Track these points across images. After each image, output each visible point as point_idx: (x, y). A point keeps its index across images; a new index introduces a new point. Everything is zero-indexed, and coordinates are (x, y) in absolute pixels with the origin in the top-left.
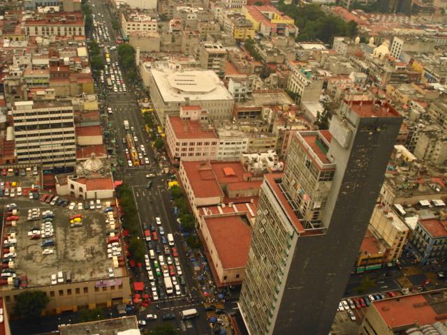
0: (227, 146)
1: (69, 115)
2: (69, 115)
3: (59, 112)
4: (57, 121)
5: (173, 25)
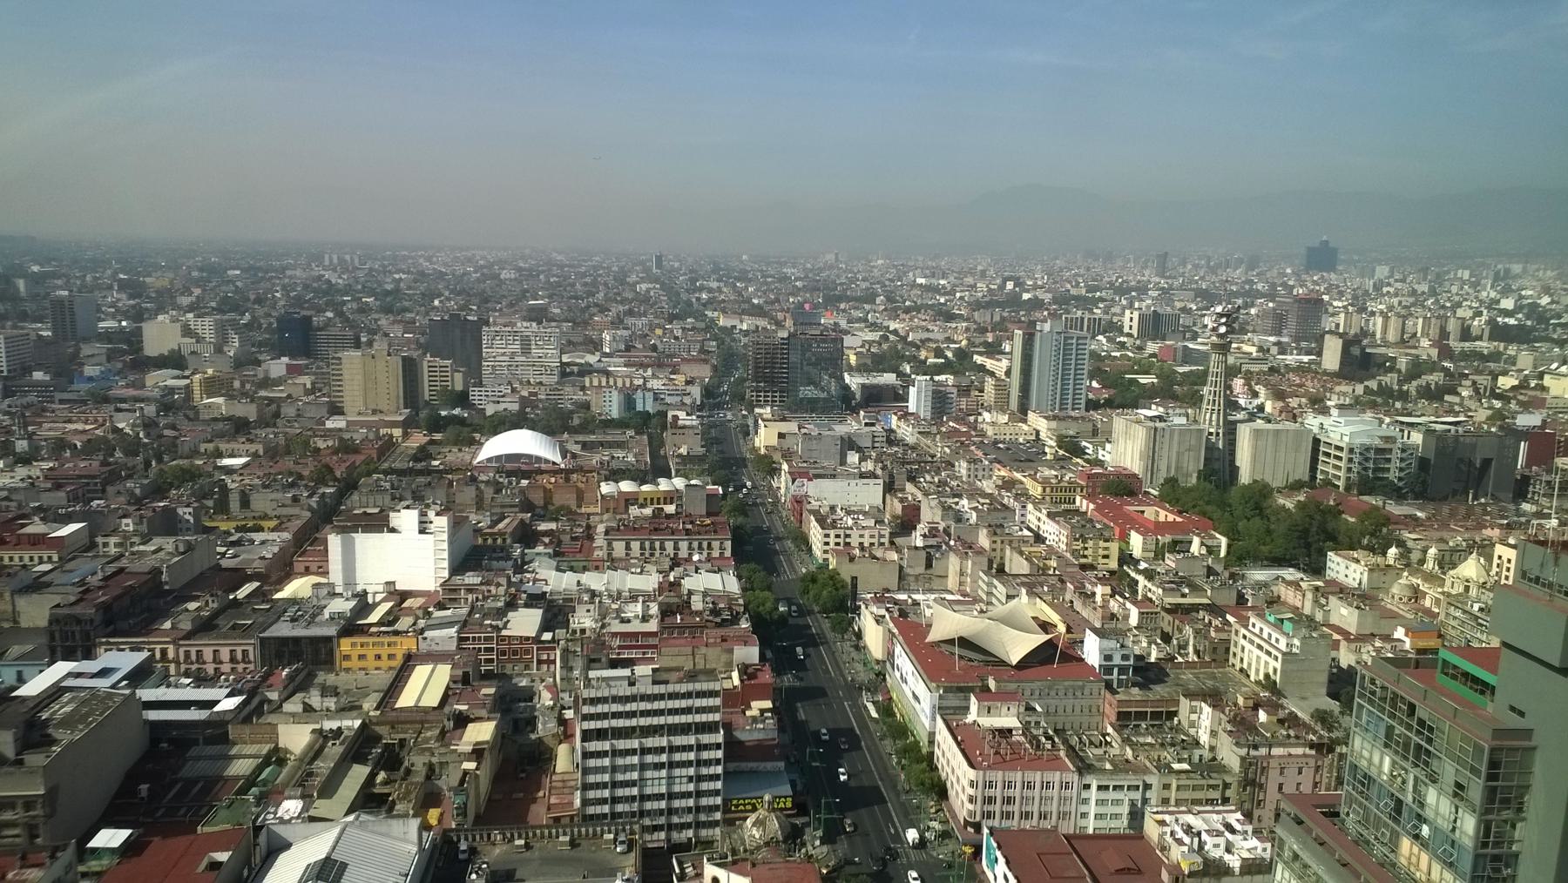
0: (1103, 795)
1: (711, 702)
2: (711, 702)
3: (688, 695)
4: (683, 719)
5: (924, 536)
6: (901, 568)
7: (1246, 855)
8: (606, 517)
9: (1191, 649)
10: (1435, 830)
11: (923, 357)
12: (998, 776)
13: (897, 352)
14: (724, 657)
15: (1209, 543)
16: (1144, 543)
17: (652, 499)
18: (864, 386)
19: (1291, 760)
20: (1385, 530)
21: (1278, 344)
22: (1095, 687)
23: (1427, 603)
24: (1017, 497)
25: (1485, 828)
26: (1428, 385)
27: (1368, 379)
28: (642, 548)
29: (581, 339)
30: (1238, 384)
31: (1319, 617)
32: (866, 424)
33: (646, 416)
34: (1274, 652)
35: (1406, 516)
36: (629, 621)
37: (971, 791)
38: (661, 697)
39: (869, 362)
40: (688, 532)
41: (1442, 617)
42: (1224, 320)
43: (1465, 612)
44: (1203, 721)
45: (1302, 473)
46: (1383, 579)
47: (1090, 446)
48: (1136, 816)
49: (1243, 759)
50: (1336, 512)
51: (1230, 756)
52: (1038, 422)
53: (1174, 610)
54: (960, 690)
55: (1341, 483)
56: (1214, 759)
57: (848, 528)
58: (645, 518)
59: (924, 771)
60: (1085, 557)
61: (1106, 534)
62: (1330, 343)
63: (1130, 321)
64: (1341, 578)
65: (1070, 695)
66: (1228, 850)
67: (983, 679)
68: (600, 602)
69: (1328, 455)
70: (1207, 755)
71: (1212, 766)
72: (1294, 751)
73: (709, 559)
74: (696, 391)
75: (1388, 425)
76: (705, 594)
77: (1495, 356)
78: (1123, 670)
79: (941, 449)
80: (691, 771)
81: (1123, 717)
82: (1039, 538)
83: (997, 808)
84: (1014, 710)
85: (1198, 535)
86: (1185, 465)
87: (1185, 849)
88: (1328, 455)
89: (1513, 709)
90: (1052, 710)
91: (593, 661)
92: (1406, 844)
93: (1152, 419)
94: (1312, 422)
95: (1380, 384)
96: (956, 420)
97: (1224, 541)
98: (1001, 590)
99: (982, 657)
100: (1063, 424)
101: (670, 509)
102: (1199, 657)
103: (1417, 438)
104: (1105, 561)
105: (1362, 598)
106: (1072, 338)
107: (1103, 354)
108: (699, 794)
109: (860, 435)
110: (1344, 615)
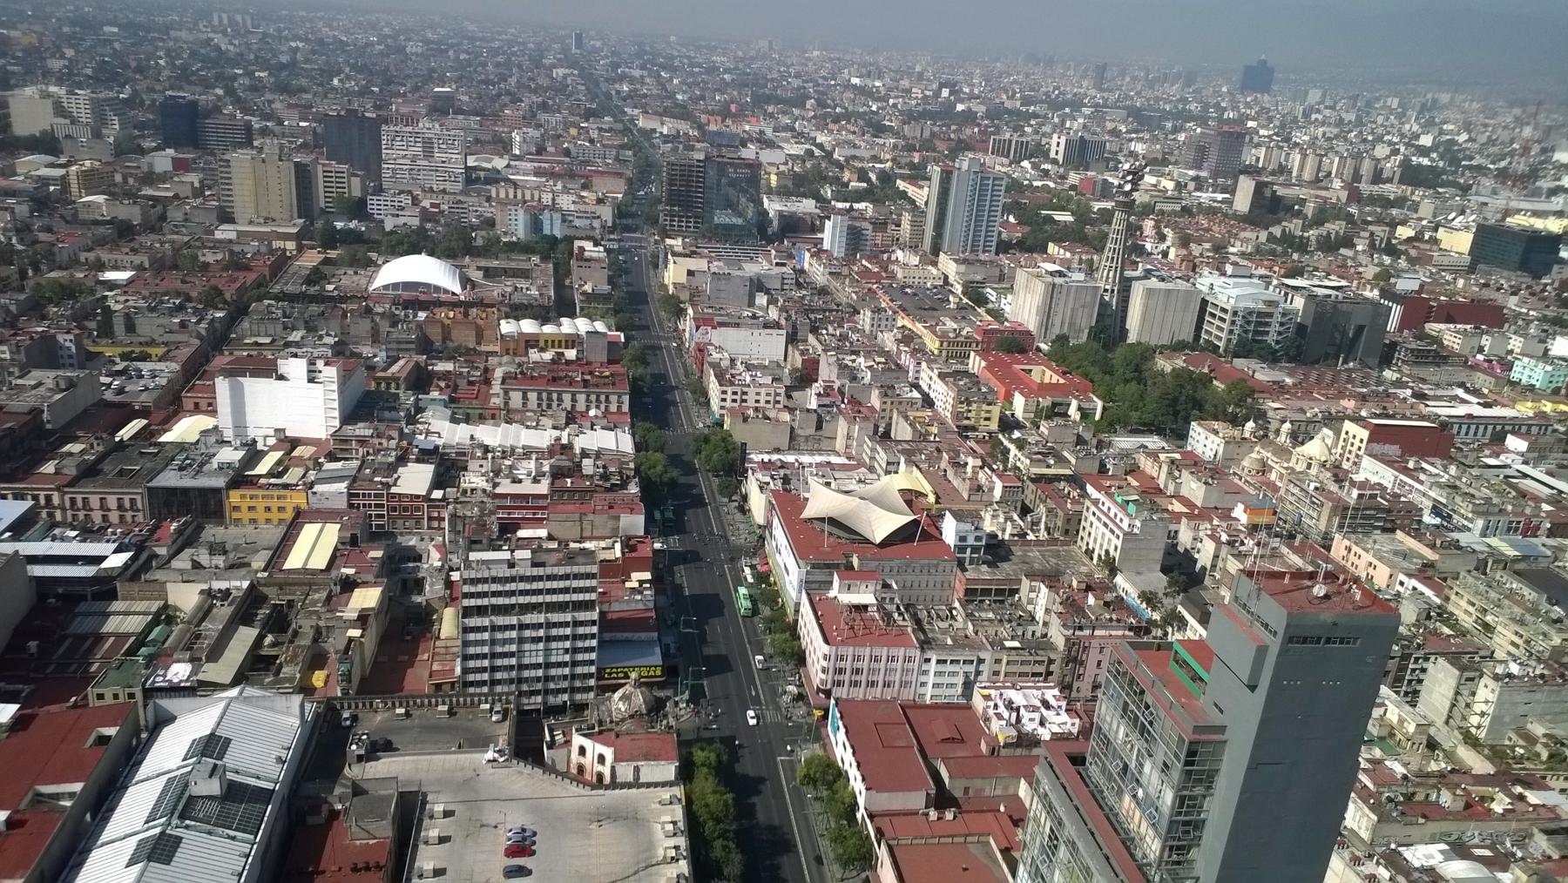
0: (941, 668)
3: (566, 577)
4: (561, 598)
5: (819, 395)
6: (792, 429)
7: (1056, 729)
8: (505, 359)
9: (1042, 526)
10: (1146, 794)
11: (846, 179)
12: (849, 651)
13: (820, 172)
14: (611, 524)
15: (1085, 405)
16: (1026, 405)
17: (553, 341)
18: (780, 212)
19: (1109, 641)
20: (1249, 400)
21: (1196, 179)
22: (948, 566)
23: (1273, 476)
24: (914, 352)
25: (1181, 800)
26: (1329, 233)
27: (1272, 225)
28: (540, 398)
29: (489, 138)
30: (1148, 225)
31: (1171, 490)
32: (777, 264)
33: (553, 241)
34: (1117, 531)
35: (1274, 382)
36: (520, 481)
37: (825, 664)
38: (540, 578)
39: (790, 184)
40: (586, 383)
41: (1282, 492)
42: (1129, 178)
43: (1302, 490)
44: (1040, 600)
45: (1187, 334)
46: (1238, 450)
48: (968, 686)
49: (1068, 639)
50: (1206, 380)
51: (1058, 636)
52: (948, 265)
53: (1038, 479)
54: (828, 566)
55: (1221, 344)
56: (1046, 635)
57: (745, 386)
58: (544, 364)
59: (786, 641)
60: (968, 418)
61: (990, 397)
62: (1245, 185)
63: (1057, 145)
64: (1199, 450)
65: (925, 571)
66: (1042, 724)
67: (848, 556)
68: (493, 458)
69: (1213, 316)
70: (1039, 630)
71: (1044, 643)
72: (1114, 633)
73: (607, 412)
74: (607, 213)
75: (1276, 287)
76: (598, 454)
77: (1400, 202)
78: (975, 549)
79: (846, 293)
80: (568, 644)
81: (970, 593)
82: (928, 402)
83: (846, 677)
84: (871, 588)
85: (1076, 398)
86: (1078, 321)
87: (1004, 723)
89: (1216, 705)
90: (908, 584)
91: (475, 542)
92: (1127, 799)
93: (1052, 274)
94: (1207, 280)
95: (1284, 231)
96: (869, 259)
97: (1100, 404)
98: (882, 457)
99: (846, 535)
100: (972, 268)
101: (571, 354)
102: (1049, 534)
103: (1299, 303)
104: (987, 423)
105: (1212, 472)
106: (988, 178)
107: (1026, 183)
108: (575, 664)
109: (770, 277)
110: (1193, 488)
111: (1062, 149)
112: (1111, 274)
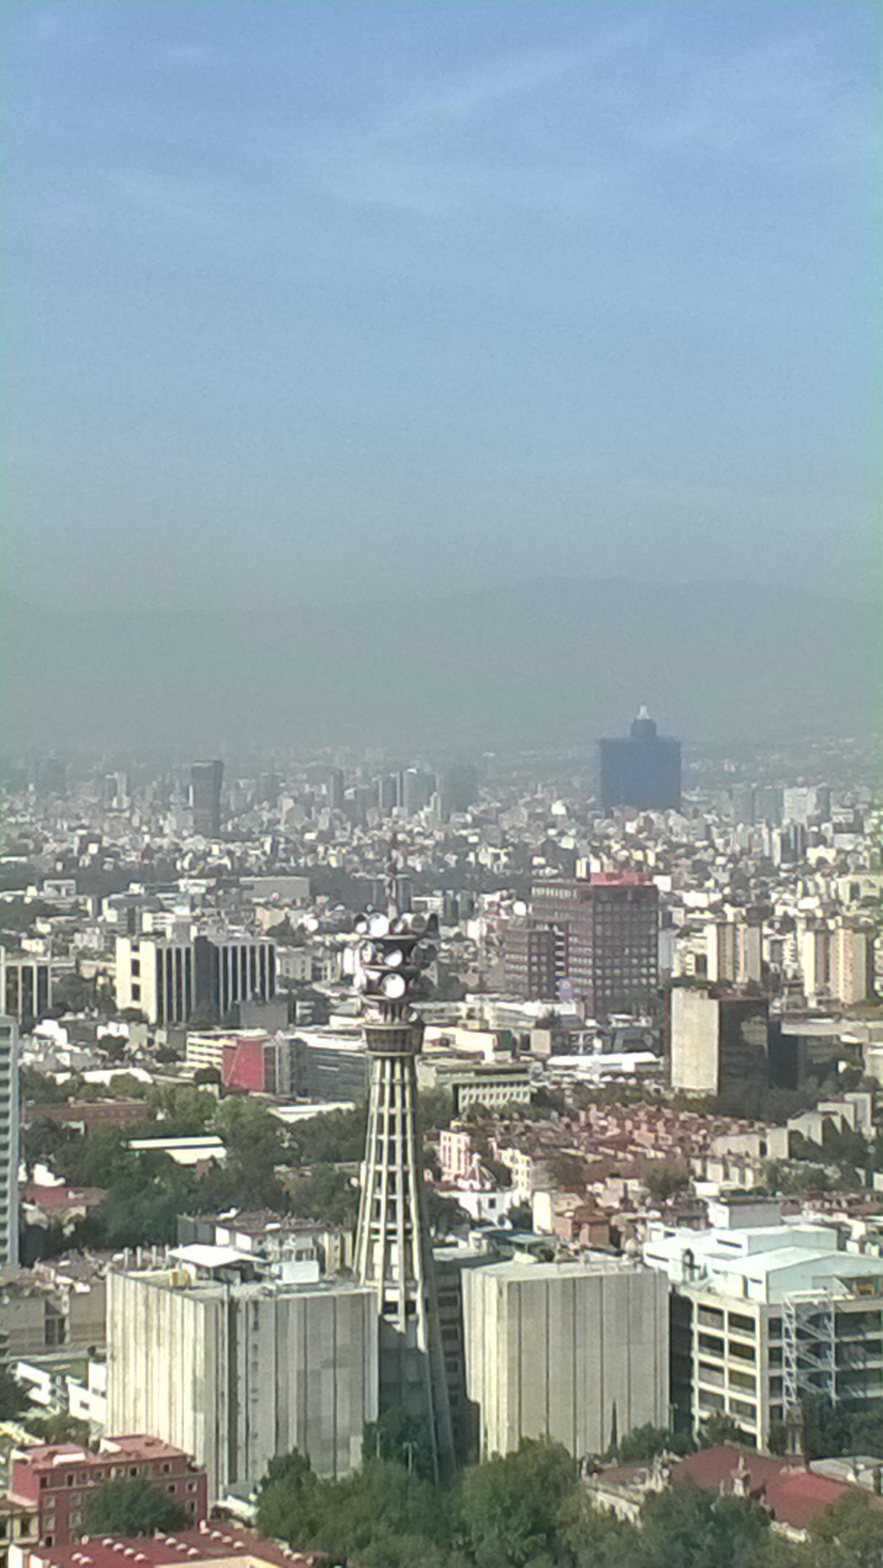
21: (550, 1022)
27: (795, 1114)
42: (395, 959)
47: (41, 1377)
55: (756, 1428)
62: (687, 1014)
69: (713, 1344)
75: (862, 1243)
86: (326, 1412)
88: (713, 1344)
93: (219, 1274)
95: (828, 1126)
107: (62, 1078)
111: (148, 979)
112: (396, 1252)
